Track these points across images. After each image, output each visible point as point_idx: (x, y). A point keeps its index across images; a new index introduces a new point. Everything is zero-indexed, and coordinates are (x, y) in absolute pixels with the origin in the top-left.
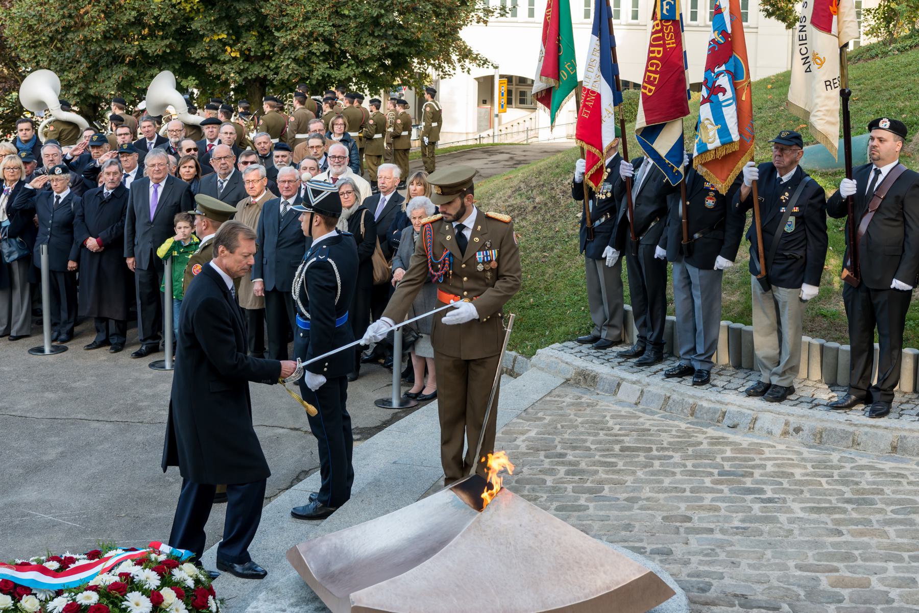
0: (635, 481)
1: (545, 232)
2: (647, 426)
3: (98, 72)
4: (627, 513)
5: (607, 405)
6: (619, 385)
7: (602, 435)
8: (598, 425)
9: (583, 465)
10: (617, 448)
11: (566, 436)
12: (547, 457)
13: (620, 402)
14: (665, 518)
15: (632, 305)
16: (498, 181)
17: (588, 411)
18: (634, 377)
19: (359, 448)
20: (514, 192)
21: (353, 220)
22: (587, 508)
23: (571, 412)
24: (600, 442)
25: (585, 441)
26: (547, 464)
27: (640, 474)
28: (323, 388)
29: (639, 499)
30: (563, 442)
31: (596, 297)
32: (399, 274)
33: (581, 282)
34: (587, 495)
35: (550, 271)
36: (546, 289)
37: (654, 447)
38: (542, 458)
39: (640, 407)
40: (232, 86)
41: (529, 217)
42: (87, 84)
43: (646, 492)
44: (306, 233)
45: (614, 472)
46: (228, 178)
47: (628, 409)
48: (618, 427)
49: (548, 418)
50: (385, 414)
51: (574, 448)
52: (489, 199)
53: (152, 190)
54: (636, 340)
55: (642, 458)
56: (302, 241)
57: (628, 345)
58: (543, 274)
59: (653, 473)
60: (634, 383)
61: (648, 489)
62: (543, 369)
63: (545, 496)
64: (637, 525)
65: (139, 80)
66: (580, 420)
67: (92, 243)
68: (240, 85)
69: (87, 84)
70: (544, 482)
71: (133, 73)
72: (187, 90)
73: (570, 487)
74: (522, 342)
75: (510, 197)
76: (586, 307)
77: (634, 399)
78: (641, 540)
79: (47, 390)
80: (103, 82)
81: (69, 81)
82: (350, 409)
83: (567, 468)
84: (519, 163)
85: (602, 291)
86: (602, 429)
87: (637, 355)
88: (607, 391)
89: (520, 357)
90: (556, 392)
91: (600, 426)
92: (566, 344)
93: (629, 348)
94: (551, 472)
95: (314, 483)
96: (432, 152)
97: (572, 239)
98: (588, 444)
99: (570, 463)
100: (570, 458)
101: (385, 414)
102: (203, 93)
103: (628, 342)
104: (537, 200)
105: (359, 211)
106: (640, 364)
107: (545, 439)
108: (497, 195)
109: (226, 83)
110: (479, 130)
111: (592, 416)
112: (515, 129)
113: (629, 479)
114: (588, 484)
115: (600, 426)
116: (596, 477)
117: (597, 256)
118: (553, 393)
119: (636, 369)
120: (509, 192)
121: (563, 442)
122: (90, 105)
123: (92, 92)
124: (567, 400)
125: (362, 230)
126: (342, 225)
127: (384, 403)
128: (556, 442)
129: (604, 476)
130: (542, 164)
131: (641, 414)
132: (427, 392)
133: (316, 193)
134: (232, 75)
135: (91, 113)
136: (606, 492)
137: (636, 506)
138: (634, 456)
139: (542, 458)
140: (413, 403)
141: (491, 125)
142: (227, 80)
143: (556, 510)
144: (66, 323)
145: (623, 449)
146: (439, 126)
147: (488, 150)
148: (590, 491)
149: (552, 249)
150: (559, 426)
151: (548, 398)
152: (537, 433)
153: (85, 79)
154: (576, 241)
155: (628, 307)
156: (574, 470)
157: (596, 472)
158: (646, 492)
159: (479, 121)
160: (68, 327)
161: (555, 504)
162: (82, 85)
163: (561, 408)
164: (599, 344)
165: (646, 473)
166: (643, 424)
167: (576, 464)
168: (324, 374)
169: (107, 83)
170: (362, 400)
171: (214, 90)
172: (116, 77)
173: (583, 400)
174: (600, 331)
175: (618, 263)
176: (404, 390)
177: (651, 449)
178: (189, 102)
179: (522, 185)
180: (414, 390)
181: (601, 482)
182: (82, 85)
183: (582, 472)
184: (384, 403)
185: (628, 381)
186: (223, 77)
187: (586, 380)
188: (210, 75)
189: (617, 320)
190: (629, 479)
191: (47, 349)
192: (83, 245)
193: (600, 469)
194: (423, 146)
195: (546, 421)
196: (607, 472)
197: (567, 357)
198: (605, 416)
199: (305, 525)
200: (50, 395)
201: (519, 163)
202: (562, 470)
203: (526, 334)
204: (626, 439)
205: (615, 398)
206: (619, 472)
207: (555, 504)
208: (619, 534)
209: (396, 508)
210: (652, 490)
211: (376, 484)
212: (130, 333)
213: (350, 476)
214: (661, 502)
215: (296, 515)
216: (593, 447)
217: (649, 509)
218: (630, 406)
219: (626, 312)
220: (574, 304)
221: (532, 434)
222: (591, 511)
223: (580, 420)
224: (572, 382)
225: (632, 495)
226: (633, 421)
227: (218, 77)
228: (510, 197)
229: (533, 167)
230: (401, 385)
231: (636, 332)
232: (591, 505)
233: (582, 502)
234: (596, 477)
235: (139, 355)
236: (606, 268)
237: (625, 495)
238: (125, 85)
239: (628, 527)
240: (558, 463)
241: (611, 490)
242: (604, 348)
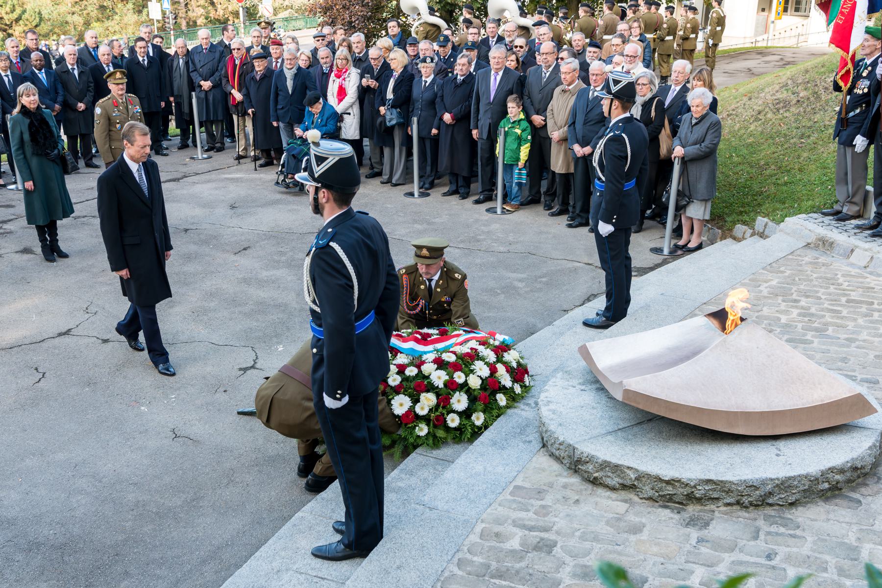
0: (855, 326)
1: (805, 122)
2: (872, 285)
4: (845, 349)
5: (840, 265)
6: (852, 251)
7: (832, 289)
8: (831, 281)
9: (813, 310)
10: (844, 299)
11: (802, 287)
12: (784, 301)
13: (852, 265)
14: (876, 357)
15: (874, 187)
16: (769, 78)
17: (823, 269)
18: (867, 246)
19: (636, 282)
20: (782, 87)
21: (646, 106)
22: (812, 342)
23: (809, 268)
24: (830, 294)
25: (817, 292)
26: (783, 306)
27: (861, 321)
28: (611, 235)
29: (857, 340)
30: (799, 291)
31: (843, 179)
32: (679, 151)
33: (831, 166)
34: (813, 333)
35: (805, 155)
36: (800, 170)
37: (876, 302)
38: (780, 301)
39: (868, 269)
41: (793, 109)
43: (864, 335)
44: (606, 115)
45: (838, 318)
47: (857, 271)
48: (847, 283)
49: (788, 273)
50: (658, 259)
51: (807, 297)
52: (759, 93)
54: (873, 215)
55: (864, 309)
56: (603, 120)
57: (865, 219)
58: (799, 157)
59: (872, 322)
60: (866, 250)
61: (865, 333)
62: (788, 234)
63: (779, 330)
64: (852, 359)
66: (815, 275)
67: (447, 117)
70: (779, 319)
73: (800, 325)
74: (774, 211)
75: (777, 91)
76: (833, 186)
77: (864, 264)
78: (854, 371)
82: (632, 252)
83: (799, 311)
84: (789, 63)
85: (849, 172)
86: (833, 284)
87: (872, 228)
88: (841, 255)
89: (770, 224)
90: (798, 252)
91: (831, 282)
92: (810, 215)
93: (866, 222)
94: (786, 312)
95: (601, 303)
96: (714, 52)
97: (827, 129)
98: (819, 295)
99: (802, 308)
100: (803, 303)
101: (658, 259)
103: (866, 216)
104: (801, 95)
105: (652, 99)
106: (874, 236)
107: (784, 287)
108: (767, 90)
110: (757, 34)
111: (825, 273)
112: (787, 34)
113: (851, 325)
114: (816, 325)
115: (831, 282)
116: (823, 320)
117: (849, 143)
118: (795, 253)
119: (870, 239)
120: (777, 87)
121: (799, 291)
124: (806, 259)
125: (653, 114)
126: (636, 111)
127: (658, 251)
128: (793, 291)
129: (830, 320)
130: (809, 65)
131: (868, 276)
132: (691, 245)
133: (616, 82)
136: (830, 331)
137: (853, 345)
138: (857, 307)
139: (780, 301)
140: (680, 252)
141: (766, 30)
143: (787, 341)
144: (429, 176)
145: (848, 301)
146: (722, 30)
147: (761, 52)
148: (816, 330)
149: (809, 136)
150: (797, 279)
151: (790, 257)
152: (778, 283)
154: (831, 131)
155: (870, 188)
156: (805, 313)
157: (823, 316)
158: (864, 335)
159: (757, 27)
160: (431, 179)
161: (786, 337)
163: (801, 265)
164: (839, 217)
165: (865, 321)
166: (869, 283)
167: (809, 308)
168: (613, 224)
170: (640, 247)
173: (820, 260)
174: (842, 207)
175: (866, 151)
176: (673, 242)
177: (872, 303)
178: (520, 8)
179: (790, 82)
180: (681, 243)
181: (826, 324)
183: (812, 315)
184: (658, 251)
185: (861, 248)
187: (825, 245)
189: (858, 199)
190: (851, 325)
192: (441, 119)
193: (827, 314)
194: (708, 47)
195: (786, 274)
196: (832, 317)
197: (811, 225)
198: (837, 275)
199: (592, 332)
200: (418, 226)
201: (789, 63)
202: (795, 312)
203: (778, 205)
204: (852, 293)
205: (847, 261)
206: (842, 318)
207: (786, 337)
208: (839, 364)
209: (660, 326)
210: (869, 334)
211: (647, 307)
212: (472, 186)
213: (628, 301)
214: (876, 344)
215: (586, 324)
216: (823, 297)
217: (864, 348)
218: (859, 268)
219: (867, 193)
220: (822, 184)
221: (774, 283)
222: (815, 345)
223: (815, 275)
224: (812, 245)
225: (851, 336)
226: (860, 280)
228: (777, 91)
229: (801, 67)
230: (671, 238)
231: (873, 209)
232: (816, 340)
233: (809, 337)
234: (823, 320)
235: (478, 202)
236: (854, 154)
237: (846, 336)
239: (845, 360)
240: (792, 307)
241: (833, 332)
242: (844, 220)
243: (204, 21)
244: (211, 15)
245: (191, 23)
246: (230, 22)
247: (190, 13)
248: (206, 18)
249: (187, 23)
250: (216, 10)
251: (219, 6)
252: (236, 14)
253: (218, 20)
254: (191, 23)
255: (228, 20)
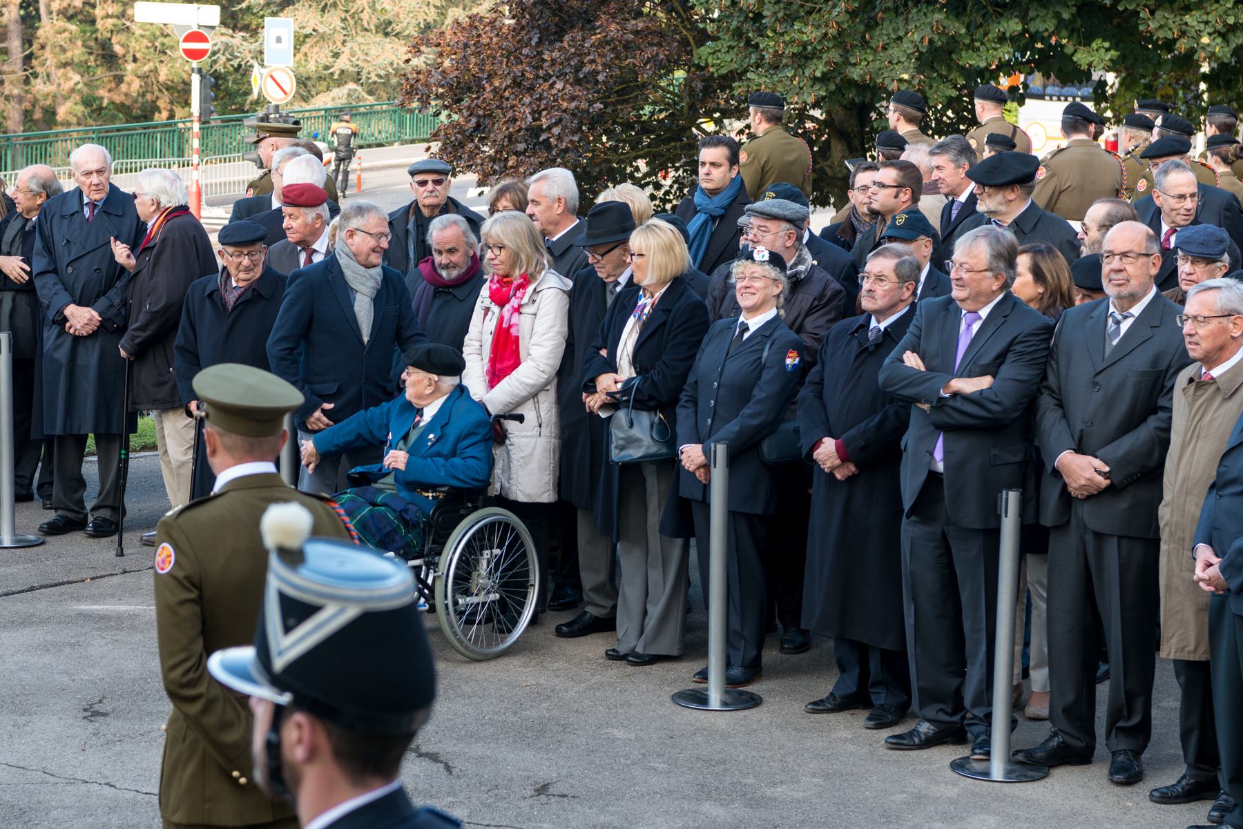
3: (872, 25)
40: (1205, 68)
42: (846, 53)
46: (1136, 310)
53: (963, 326)
65: (970, 47)
68: (1223, 66)
69: (846, 53)
71: (957, 28)
72: (1088, 75)
79: (709, 797)
80: (884, 49)
81: (804, 45)
102: (1127, 84)
109: (1188, 61)
122: (850, 107)
123: (855, 74)
134: (1205, 40)
135: (852, 126)
142: (1192, 51)
153: (840, 40)
162: (834, 55)
169: (895, 52)
171: (1156, 76)
172: (916, 37)
182: (834, 55)
186: (1183, 45)
188: (1150, 39)
191: (715, 696)
227: (1169, 45)
238: (935, 58)
243: (80, 109)
244: (102, 92)
245: (38, 115)
246: (161, 117)
247: (39, 86)
248: (87, 102)
249: (27, 114)
250: (119, 80)
251: (130, 67)
252: (180, 93)
253: (122, 108)
254: (38, 115)
255: (155, 108)
